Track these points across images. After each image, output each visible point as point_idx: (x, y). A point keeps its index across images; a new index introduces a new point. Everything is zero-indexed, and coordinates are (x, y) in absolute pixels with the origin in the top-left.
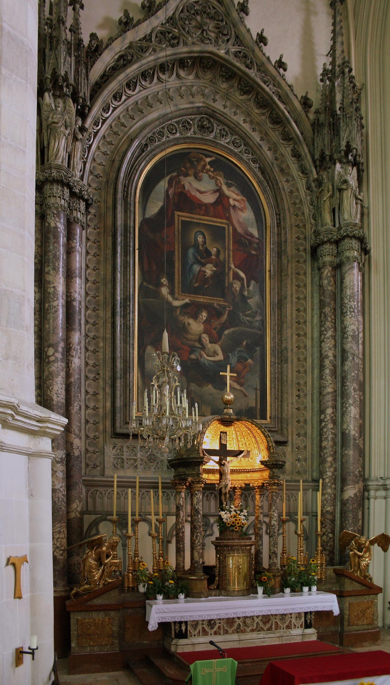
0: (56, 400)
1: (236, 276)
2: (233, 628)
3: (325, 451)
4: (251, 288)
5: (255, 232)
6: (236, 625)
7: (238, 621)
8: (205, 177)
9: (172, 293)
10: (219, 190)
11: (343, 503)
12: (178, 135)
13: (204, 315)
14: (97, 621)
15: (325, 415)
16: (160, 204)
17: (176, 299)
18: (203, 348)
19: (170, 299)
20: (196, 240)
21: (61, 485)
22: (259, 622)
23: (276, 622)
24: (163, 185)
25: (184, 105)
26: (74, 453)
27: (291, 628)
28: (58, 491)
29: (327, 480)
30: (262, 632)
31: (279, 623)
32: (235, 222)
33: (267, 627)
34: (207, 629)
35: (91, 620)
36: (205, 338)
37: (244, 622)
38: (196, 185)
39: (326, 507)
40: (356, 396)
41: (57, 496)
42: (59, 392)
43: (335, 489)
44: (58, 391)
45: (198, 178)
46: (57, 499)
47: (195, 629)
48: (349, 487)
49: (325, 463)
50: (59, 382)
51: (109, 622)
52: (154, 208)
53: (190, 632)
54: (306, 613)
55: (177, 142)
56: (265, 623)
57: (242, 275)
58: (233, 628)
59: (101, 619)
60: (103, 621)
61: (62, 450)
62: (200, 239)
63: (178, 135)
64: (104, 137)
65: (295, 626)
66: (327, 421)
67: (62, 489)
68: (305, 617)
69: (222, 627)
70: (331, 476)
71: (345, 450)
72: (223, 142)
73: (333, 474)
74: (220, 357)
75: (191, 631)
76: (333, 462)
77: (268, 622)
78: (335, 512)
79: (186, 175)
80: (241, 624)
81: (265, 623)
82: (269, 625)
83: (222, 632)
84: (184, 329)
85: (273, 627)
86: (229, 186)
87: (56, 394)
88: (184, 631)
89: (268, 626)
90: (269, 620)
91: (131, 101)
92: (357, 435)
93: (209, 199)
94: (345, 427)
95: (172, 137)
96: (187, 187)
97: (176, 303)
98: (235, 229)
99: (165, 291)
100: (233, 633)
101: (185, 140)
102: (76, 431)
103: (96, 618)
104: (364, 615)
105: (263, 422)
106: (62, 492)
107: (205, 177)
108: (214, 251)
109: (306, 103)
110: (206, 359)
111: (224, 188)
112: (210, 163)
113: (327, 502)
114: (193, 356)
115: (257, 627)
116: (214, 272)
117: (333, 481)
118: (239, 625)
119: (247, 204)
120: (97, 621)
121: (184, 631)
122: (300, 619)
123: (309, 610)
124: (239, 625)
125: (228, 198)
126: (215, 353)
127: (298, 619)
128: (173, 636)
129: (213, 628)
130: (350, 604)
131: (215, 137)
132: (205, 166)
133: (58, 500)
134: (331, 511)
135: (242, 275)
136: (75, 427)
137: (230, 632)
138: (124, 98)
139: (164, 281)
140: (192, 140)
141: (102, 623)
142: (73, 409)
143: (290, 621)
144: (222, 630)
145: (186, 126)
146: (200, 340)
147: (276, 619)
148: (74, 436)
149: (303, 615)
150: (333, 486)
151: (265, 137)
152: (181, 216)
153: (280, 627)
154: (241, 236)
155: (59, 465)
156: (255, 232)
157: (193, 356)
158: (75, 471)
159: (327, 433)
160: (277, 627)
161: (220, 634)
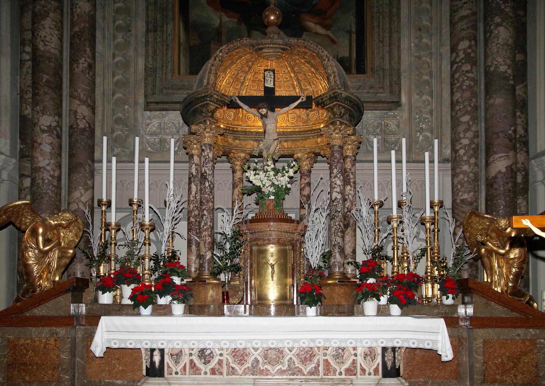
0: (42, 49)
2: (246, 366)
3: (457, 108)
6: (251, 360)
7: (256, 354)
11: (490, 184)
14: (37, 343)
15: (457, 53)
21: (47, 162)
22: (294, 359)
23: (326, 361)
26: (78, 125)
27: (355, 375)
28: (42, 170)
29: (462, 152)
30: (299, 377)
31: (332, 364)
33: (308, 369)
34: (198, 363)
35: (29, 341)
37: (265, 357)
39: (460, 194)
40: (508, 10)
41: (41, 177)
42: (48, 39)
43: (476, 164)
44: (45, 37)
46: (41, 181)
47: (177, 362)
48: (497, 156)
49: (458, 125)
50: (46, 26)
51: (55, 346)
53: (169, 367)
54: (384, 349)
56: (304, 361)
58: (246, 366)
59: (44, 341)
60: (46, 344)
61: (50, 115)
65: (363, 370)
66: (460, 61)
67: (49, 168)
68: (383, 356)
69: (225, 362)
70: (469, 145)
71: (489, 99)
73: (472, 142)
75: (171, 365)
76: (471, 123)
77: (311, 361)
78: (476, 201)
80: (259, 358)
81: (304, 361)
82: (313, 365)
83: (225, 370)
85: (321, 368)
87: (43, 41)
88: (157, 364)
89: (311, 366)
90: (312, 356)
92: (509, 71)
94: (489, 63)
100: (245, 373)
102: (82, 96)
103: (36, 339)
104: (515, 365)
106: (49, 171)
113: (462, 186)
115: (289, 366)
117: (471, 152)
118: (257, 361)
120: (37, 343)
121: (157, 364)
122: (373, 359)
123: (390, 345)
124: (257, 361)
127: (369, 358)
128: (144, 372)
129: (209, 362)
130: (485, 342)
133: (43, 183)
134: (469, 200)
136: (79, 91)
137: (240, 372)
141: (45, 347)
142: (77, 67)
143: (354, 362)
144: (225, 367)
147: (325, 354)
148: (78, 103)
149: (380, 351)
150: (472, 160)
153: (335, 371)
155: (45, 135)
158: (79, 148)
159: (461, 79)
160: (328, 370)
161: (221, 374)
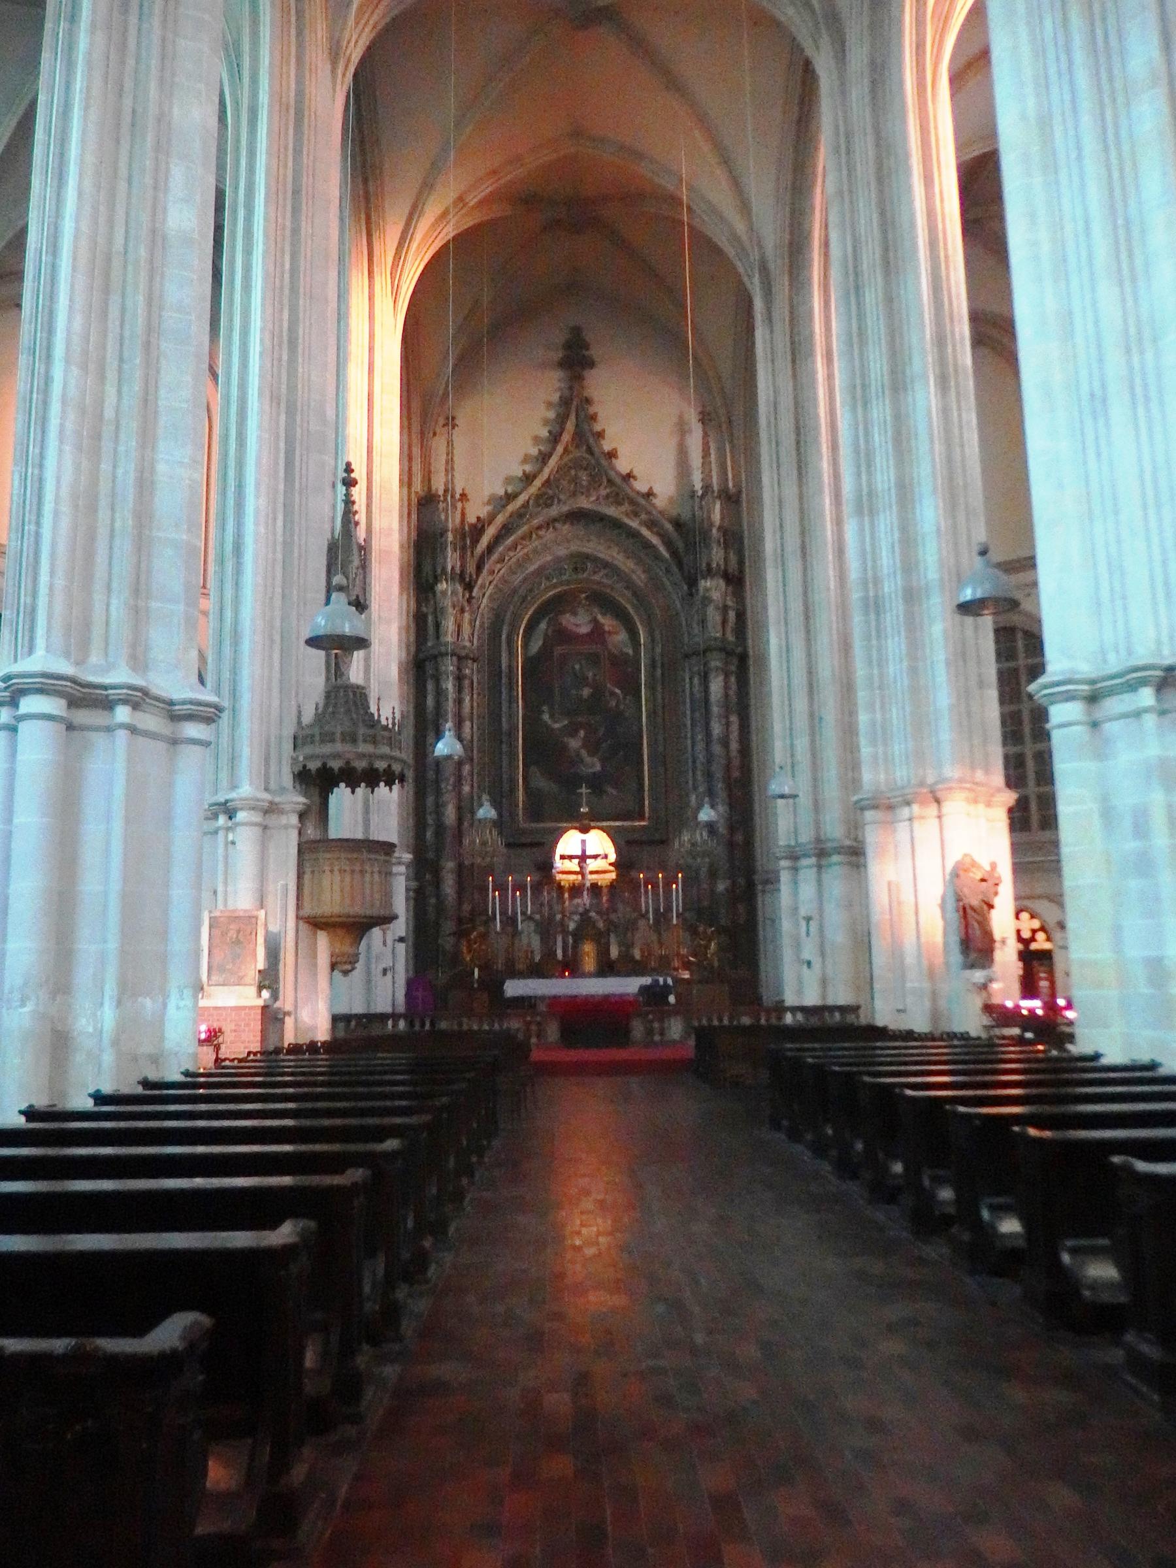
1: (613, 694)
4: (627, 702)
5: (631, 652)
8: (581, 611)
9: (552, 716)
10: (595, 621)
12: (555, 581)
13: (582, 733)
16: (540, 643)
17: (556, 722)
18: (582, 761)
19: (550, 722)
20: (573, 668)
24: (543, 626)
25: (562, 552)
32: (610, 647)
36: (584, 753)
38: (572, 619)
45: (575, 614)
52: (536, 645)
55: (555, 586)
57: (618, 691)
62: (577, 667)
63: (555, 581)
64: (491, 595)
72: (596, 577)
74: (598, 768)
79: (563, 612)
84: (565, 748)
86: (604, 614)
91: (514, 560)
93: (584, 630)
95: (548, 584)
96: (564, 623)
97: (557, 726)
98: (609, 653)
99: (546, 717)
101: (561, 584)
105: (643, 823)
107: (581, 611)
108: (590, 674)
109: (678, 524)
110: (585, 770)
111: (599, 617)
112: (587, 598)
114: (572, 771)
116: (592, 695)
119: (622, 628)
125: (603, 625)
126: (593, 765)
131: (589, 575)
132: (580, 603)
135: (618, 691)
138: (507, 558)
139: (545, 708)
140: (568, 582)
145: (561, 571)
146: (578, 755)
151: (640, 562)
152: (558, 650)
154: (615, 656)
156: (631, 652)
157: (572, 771)
